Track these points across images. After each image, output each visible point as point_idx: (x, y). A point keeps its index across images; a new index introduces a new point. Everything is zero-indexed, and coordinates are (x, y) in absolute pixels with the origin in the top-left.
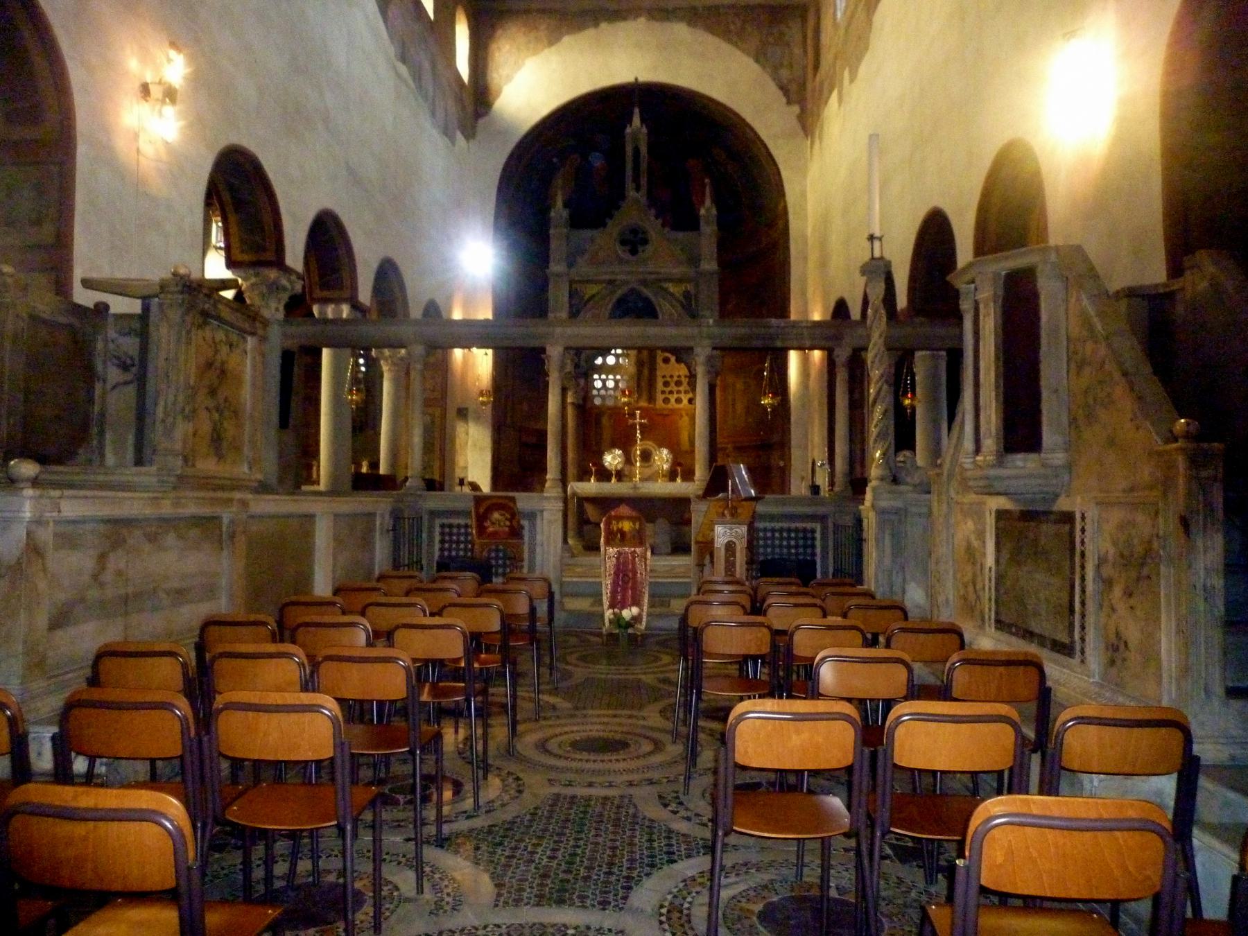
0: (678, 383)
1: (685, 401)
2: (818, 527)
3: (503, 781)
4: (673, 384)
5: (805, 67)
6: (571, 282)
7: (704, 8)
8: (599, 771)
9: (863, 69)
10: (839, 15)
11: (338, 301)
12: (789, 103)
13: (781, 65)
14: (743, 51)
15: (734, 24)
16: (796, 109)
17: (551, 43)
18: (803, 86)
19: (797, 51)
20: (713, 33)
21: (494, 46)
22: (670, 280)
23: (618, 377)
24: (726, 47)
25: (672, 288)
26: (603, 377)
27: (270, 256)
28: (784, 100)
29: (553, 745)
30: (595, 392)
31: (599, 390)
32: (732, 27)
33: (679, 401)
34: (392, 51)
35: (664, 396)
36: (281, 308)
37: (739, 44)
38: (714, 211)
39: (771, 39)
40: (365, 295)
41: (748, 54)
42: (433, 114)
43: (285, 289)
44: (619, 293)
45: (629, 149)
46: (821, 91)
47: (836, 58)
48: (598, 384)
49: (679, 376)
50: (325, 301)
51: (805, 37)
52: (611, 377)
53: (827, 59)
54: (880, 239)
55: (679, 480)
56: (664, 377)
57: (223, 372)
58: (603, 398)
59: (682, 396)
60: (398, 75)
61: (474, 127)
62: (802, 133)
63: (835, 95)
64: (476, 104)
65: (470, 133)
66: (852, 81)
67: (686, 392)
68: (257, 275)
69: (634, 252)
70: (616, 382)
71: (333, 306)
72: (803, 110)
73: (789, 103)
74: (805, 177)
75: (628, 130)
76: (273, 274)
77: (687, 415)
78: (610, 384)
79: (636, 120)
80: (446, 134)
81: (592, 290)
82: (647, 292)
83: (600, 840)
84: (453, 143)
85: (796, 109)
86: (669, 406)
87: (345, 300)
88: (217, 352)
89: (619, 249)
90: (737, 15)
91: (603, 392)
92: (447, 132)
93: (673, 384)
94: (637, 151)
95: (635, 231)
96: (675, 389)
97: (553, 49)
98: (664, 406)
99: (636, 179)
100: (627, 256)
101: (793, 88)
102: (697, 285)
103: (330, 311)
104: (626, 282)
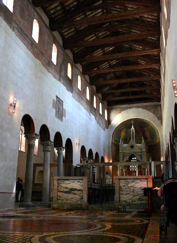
6: (123, 153)
11: (91, 159)
12: (159, 120)
16: (160, 121)
21: (111, 114)
25: (137, 153)
39: (156, 110)
40: (94, 158)
41: (152, 113)
42: (102, 128)
44: (130, 155)
48: (131, 167)
69: (132, 148)
73: (159, 120)
75: (131, 129)
76: (85, 158)
79: (133, 127)
81: (126, 154)
82: (134, 154)
85: (160, 121)
87: (91, 159)
89: (130, 148)
90: (149, 107)
92: (104, 130)
94: (133, 132)
95: (132, 145)
100: (131, 149)
101: (159, 118)
102: (142, 153)
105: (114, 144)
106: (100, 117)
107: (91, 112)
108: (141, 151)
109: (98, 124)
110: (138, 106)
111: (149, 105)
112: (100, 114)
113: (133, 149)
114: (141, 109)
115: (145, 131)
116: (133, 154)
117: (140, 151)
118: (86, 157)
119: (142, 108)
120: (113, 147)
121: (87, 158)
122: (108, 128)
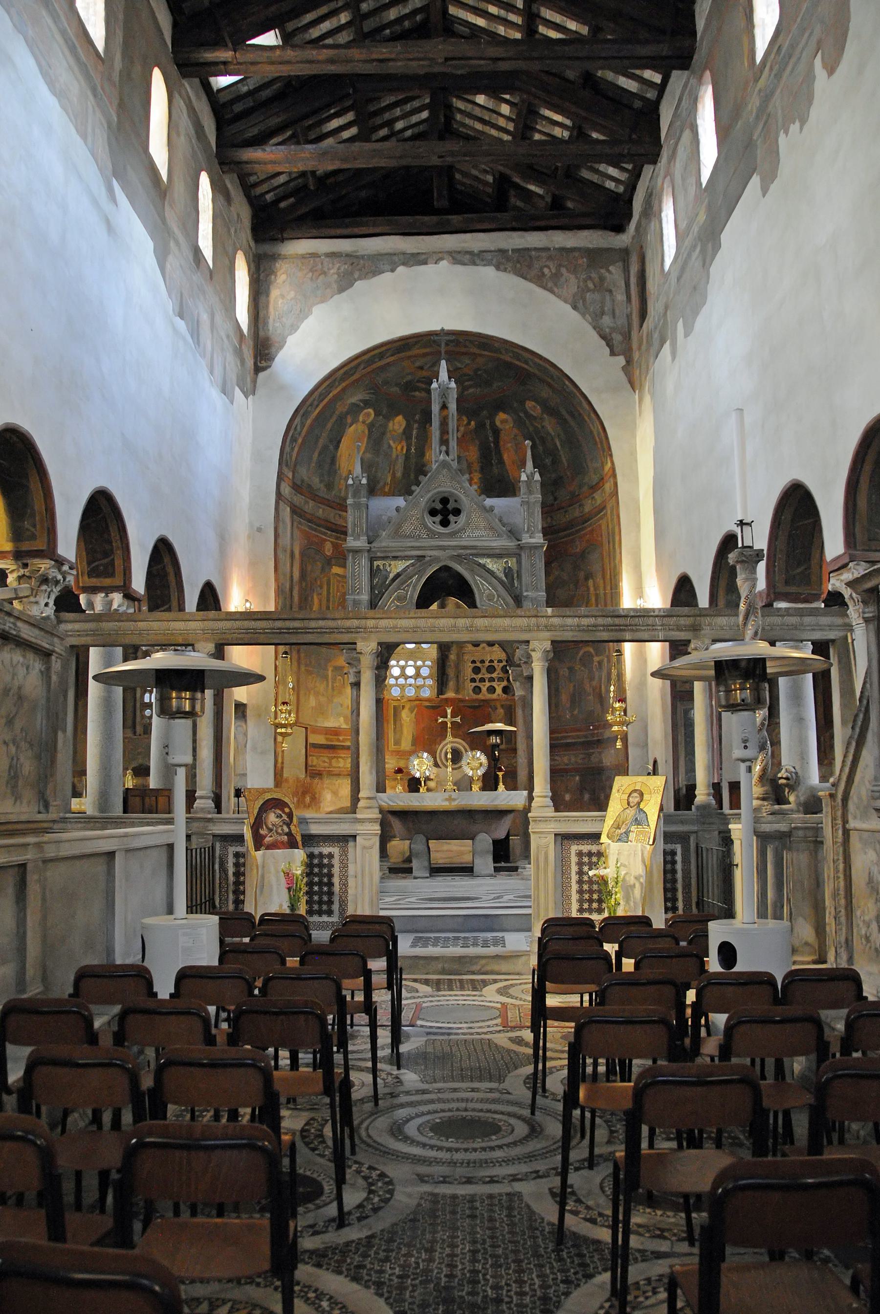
0: (491, 669)
1: (499, 690)
2: (679, 849)
3: (366, 1178)
4: (484, 670)
5: (629, 317)
6: (372, 560)
7: (512, 250)
8: (475, 1162)
9: (700, 322)
10: (668, 261)
11: (108, 590)
12: (613, 353)
13: (603, 313)
14: (559, 297)
15: (549, 268)
16: (621, 360)
17: (341, 290)
18: (627, 336)
19: (620, 297)
20: (525, 278)
22: (489, 556)
23: (419, 663)
24: (539, 291)
25: (490, 564)
26: (402, 663)
27: (40, 544)
28: (608, 350)
29: (411, 1129)
30: (392, 681)
31: (397, 678)
32: (546, 271)
33: (492, 690)
34: (170, 306)
35: (474, 684)
36: (51, 602)
37: (556, 290)
38: (537, 477)
40: (139, 584)
41: (566, 301)
42: (212, 372)
43: (57, 582)
45: (435, 408)
46: (650, 344)
47: (666, 308)
48: (396, 671)
49: (492, 661)
50: (93, 590)
51: (627, 285)
52: (411, 663)
53: (654, 308)
54: (749, 524)
55: (501, 787)
56: (474, 662)
57: (20, 698)
58: (402, 687)
59: (494, 684)
60: (175, 330)
61: (254, 382)
62: (629, 386)
63: (667, 346)
64: (255, 357)
65: (250, 391)
66: (686, 335)
67: (500, 679)
68: (25, 566)
69: (445, 523)
70: (418, 669)
71: (103, 595)
72: (629, 362)
73: (613, 353)
74: (634, 436)
75: (434, 385)
76: (44, 565)
77: (502, 706)
78: (410, 671)
79: (443, 375)
80: (224, 392)
83: (500, 1251)
84: (232, 403)
85: (621, 360)
86: (480, 697)
88: (14, 675)
89: (429, 520)
90: (550, 258)
91: (401, 681)
92: (225, 391)
93: (484, 670)
94: (444, 407)
95: (445, 501)
96: (488, 676)
97: (344, 294)
98: (475, 696)
99: (444, 442)
101: (617, 338)
102: (519, 562)
103: (99, 599)
104: (436, 559)
105: (296, 511)
106: (197, 278)
107: (116, 175)
108: (511, 544)
109: (181, 316)
110: (470, 253)
111: (547, 249)
112: (197, 252)
113: (452, 527)
114: (489, 272)
115: (496, 432)
116: (446, 568)
117: (505, 543)
118: (50, 552)
119: (498, 268)
120: (288, 520)
121: (60, 562)
122: (254, 394)
